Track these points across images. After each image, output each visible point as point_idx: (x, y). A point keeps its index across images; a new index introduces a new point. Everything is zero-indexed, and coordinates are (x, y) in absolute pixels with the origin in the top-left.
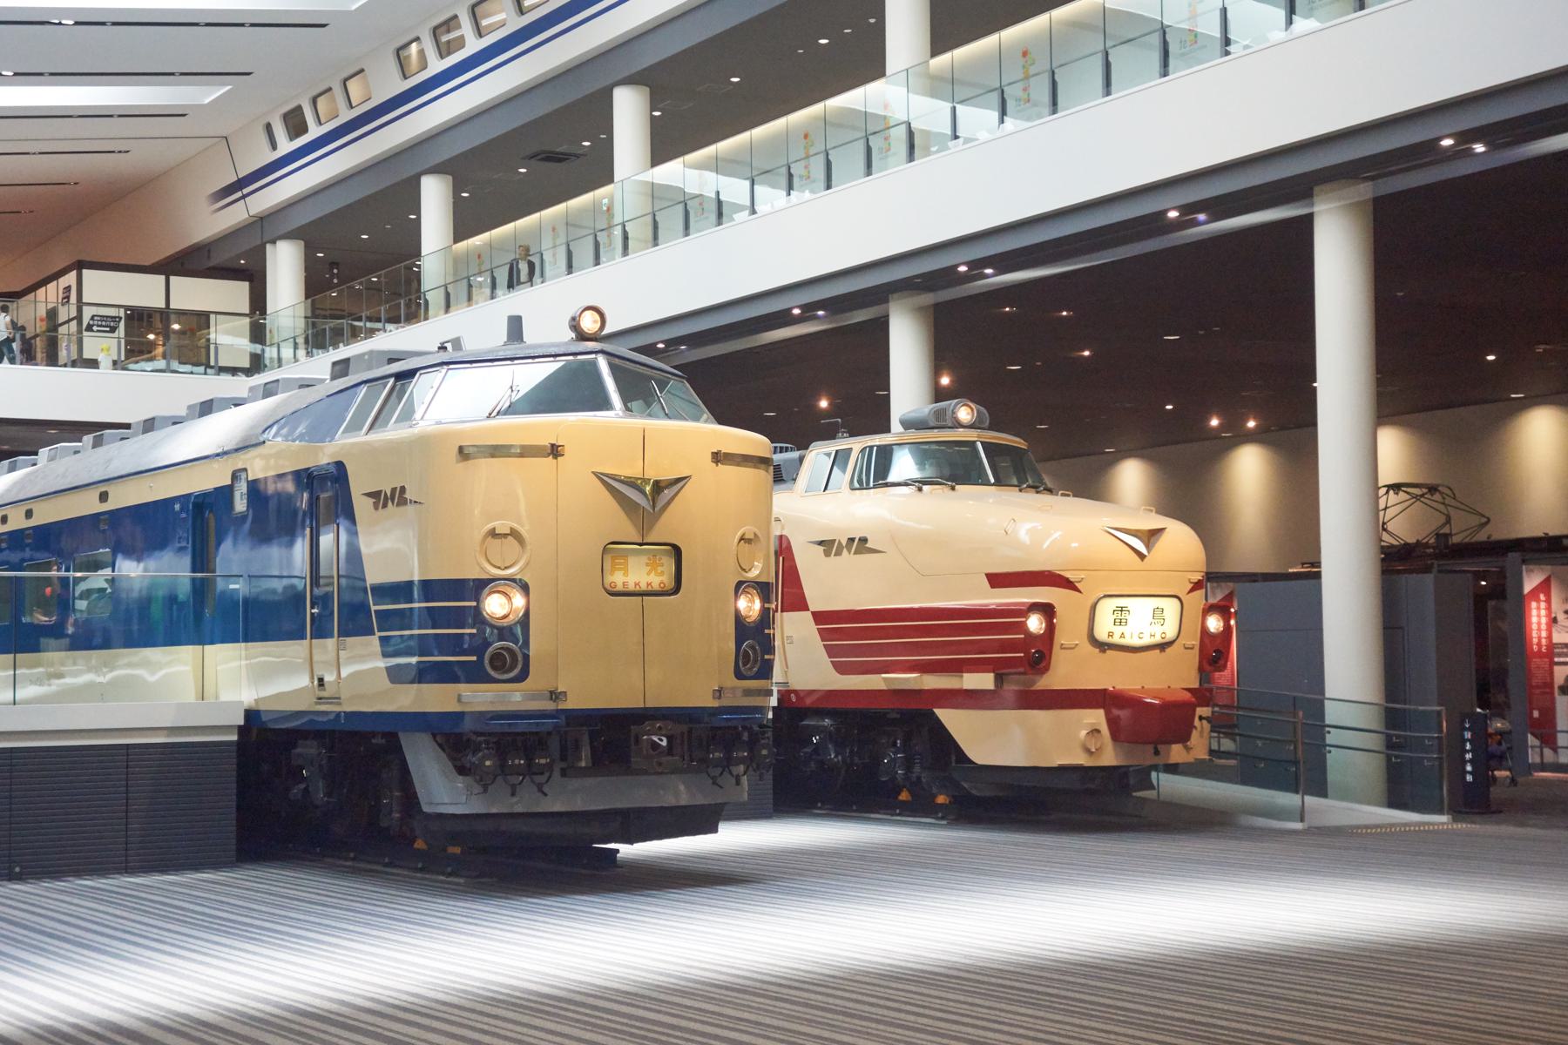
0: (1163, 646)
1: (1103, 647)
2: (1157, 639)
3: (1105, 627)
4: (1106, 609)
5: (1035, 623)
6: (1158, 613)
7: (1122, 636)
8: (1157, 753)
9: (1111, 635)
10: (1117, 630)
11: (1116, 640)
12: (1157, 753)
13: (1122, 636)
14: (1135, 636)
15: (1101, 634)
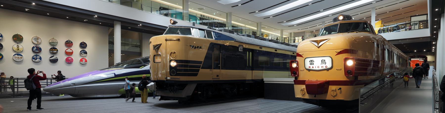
0: (328, 70)
1: (309, 70)
2: (324, 68)
3: (308, 65)
4: (308, 61)
5: (294, 65)
6: (323, 62)
7: (313, 67)
8: (315, 96)
9: (310, 67)
10: (311, 66)
11: (311, 68)
12: (315, 96)
13: (313, 67)
14: (317, 67)
15: (307, 67)
